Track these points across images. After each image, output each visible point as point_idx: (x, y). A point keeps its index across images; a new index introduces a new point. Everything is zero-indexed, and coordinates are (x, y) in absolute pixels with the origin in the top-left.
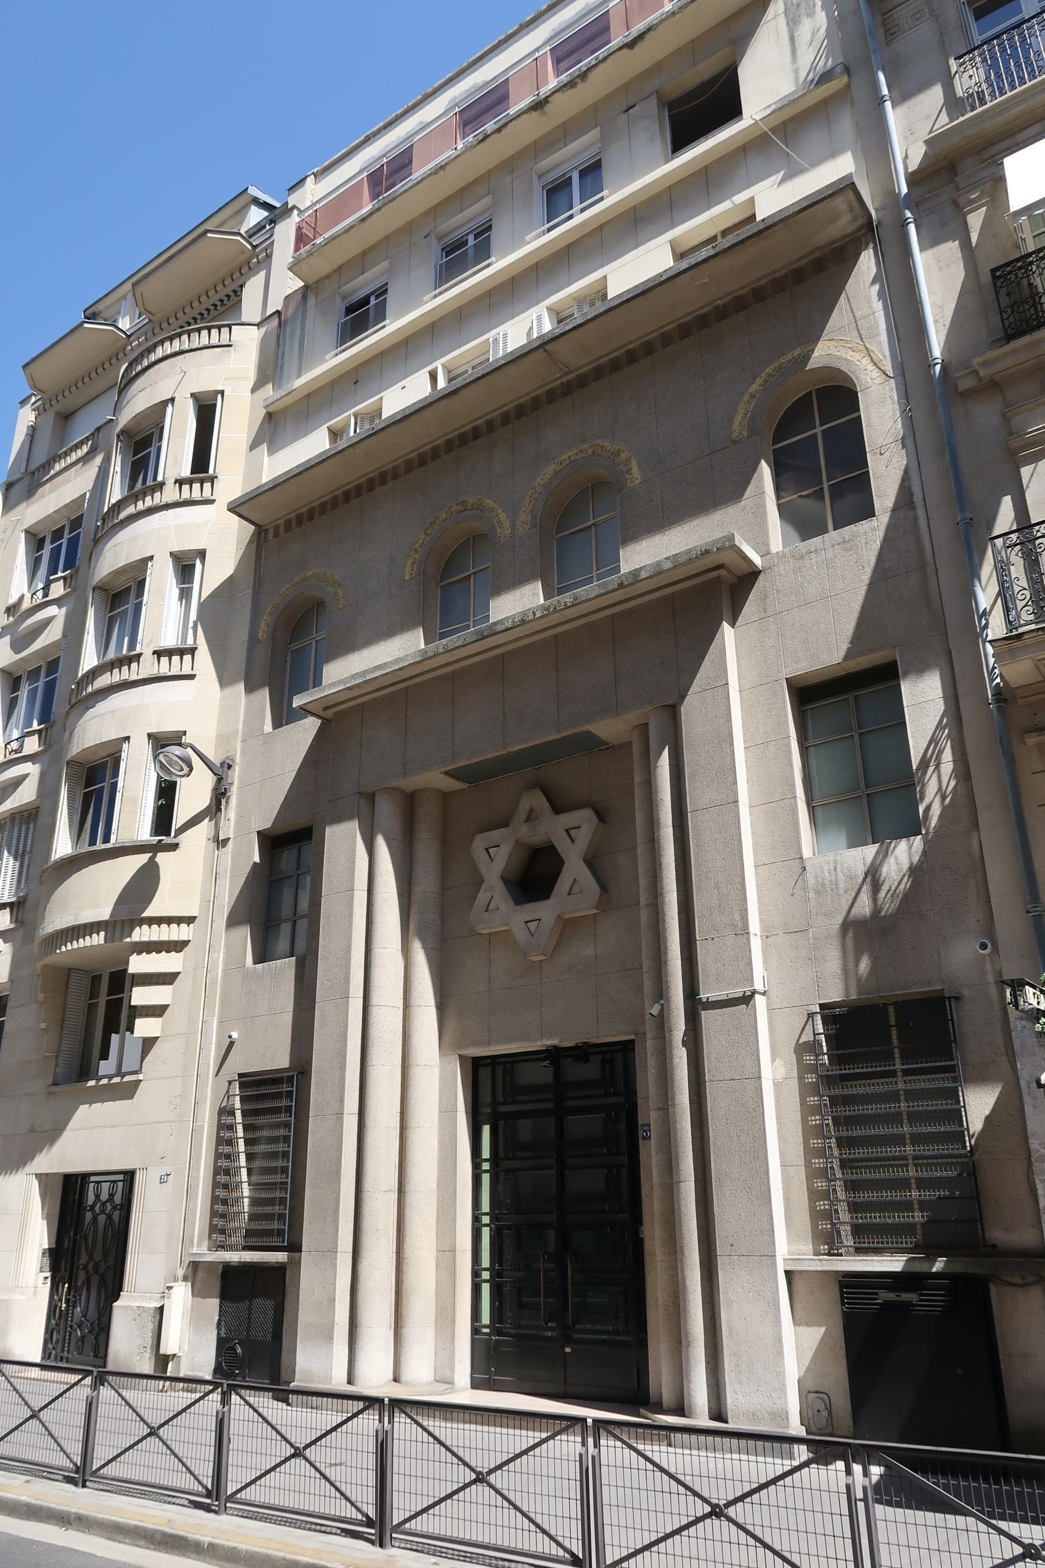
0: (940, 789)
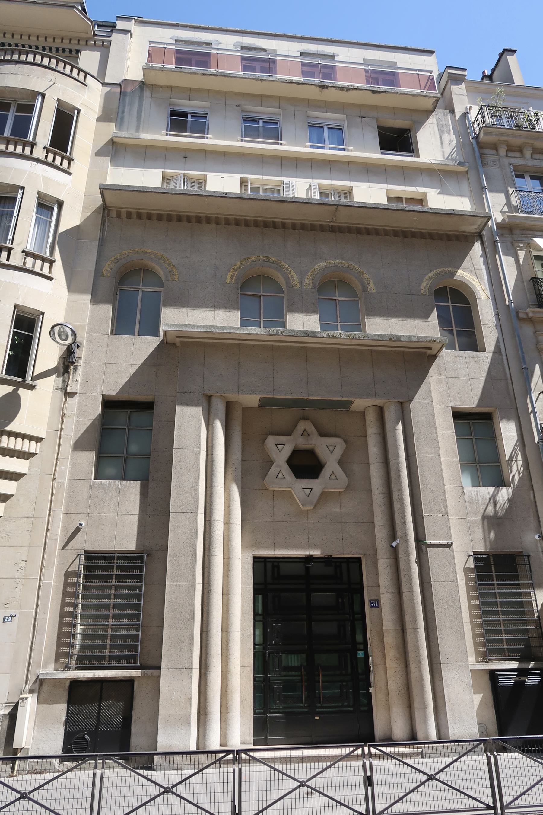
0: (518, 469)
